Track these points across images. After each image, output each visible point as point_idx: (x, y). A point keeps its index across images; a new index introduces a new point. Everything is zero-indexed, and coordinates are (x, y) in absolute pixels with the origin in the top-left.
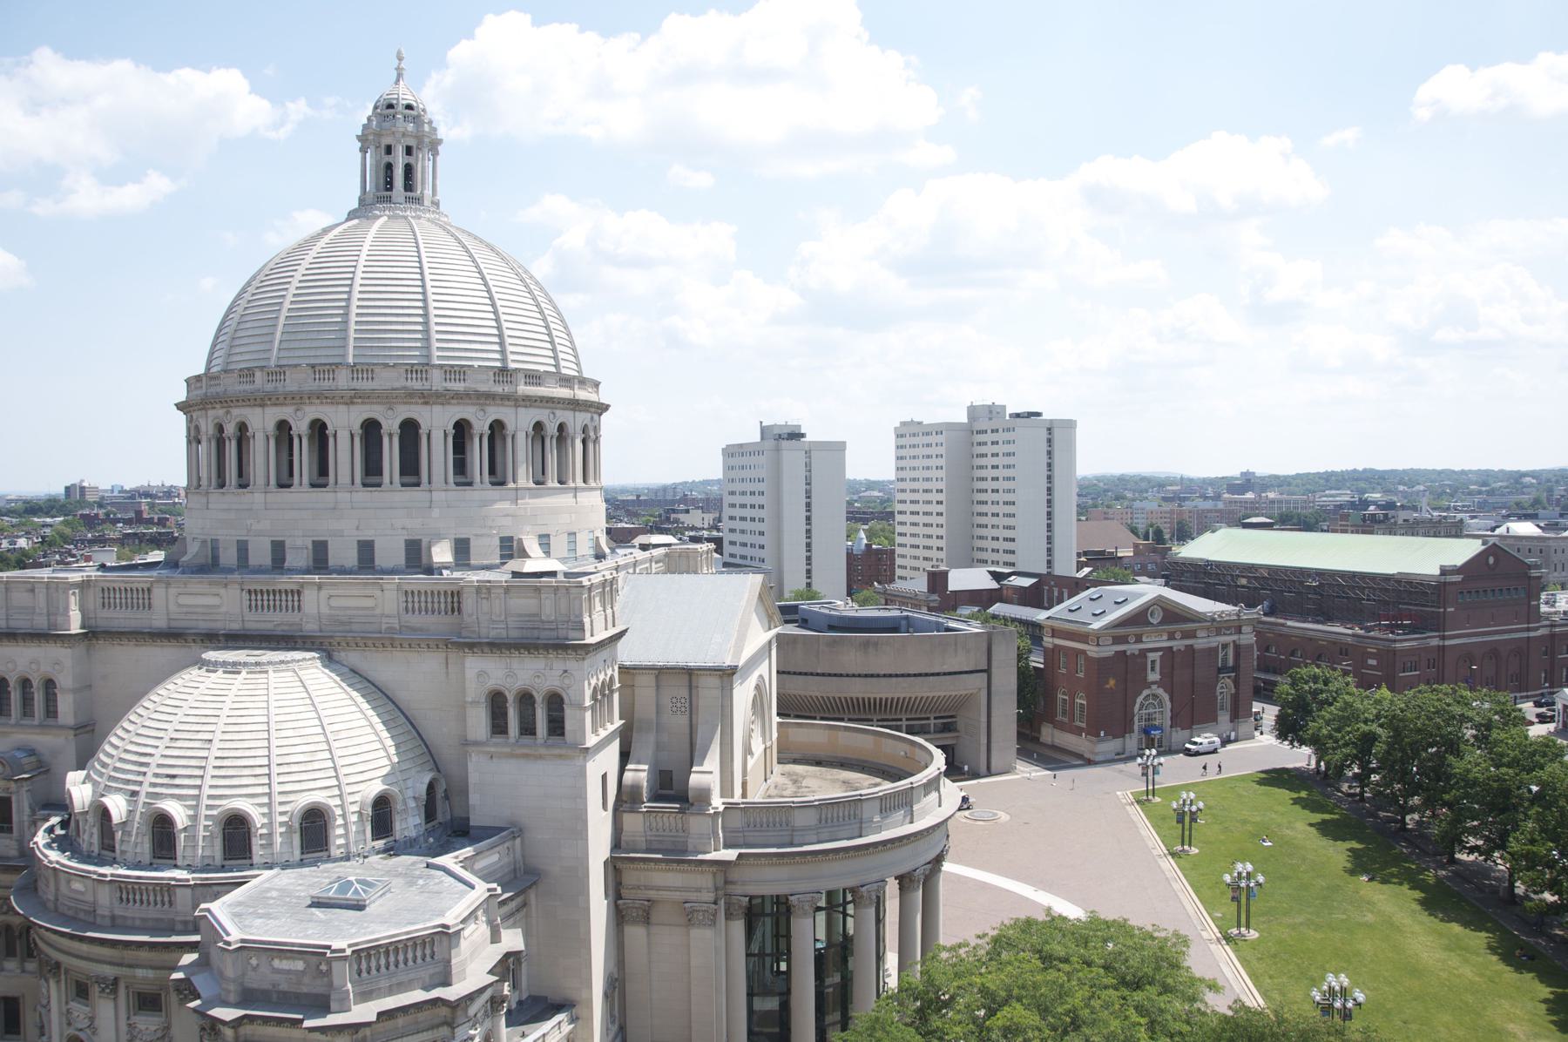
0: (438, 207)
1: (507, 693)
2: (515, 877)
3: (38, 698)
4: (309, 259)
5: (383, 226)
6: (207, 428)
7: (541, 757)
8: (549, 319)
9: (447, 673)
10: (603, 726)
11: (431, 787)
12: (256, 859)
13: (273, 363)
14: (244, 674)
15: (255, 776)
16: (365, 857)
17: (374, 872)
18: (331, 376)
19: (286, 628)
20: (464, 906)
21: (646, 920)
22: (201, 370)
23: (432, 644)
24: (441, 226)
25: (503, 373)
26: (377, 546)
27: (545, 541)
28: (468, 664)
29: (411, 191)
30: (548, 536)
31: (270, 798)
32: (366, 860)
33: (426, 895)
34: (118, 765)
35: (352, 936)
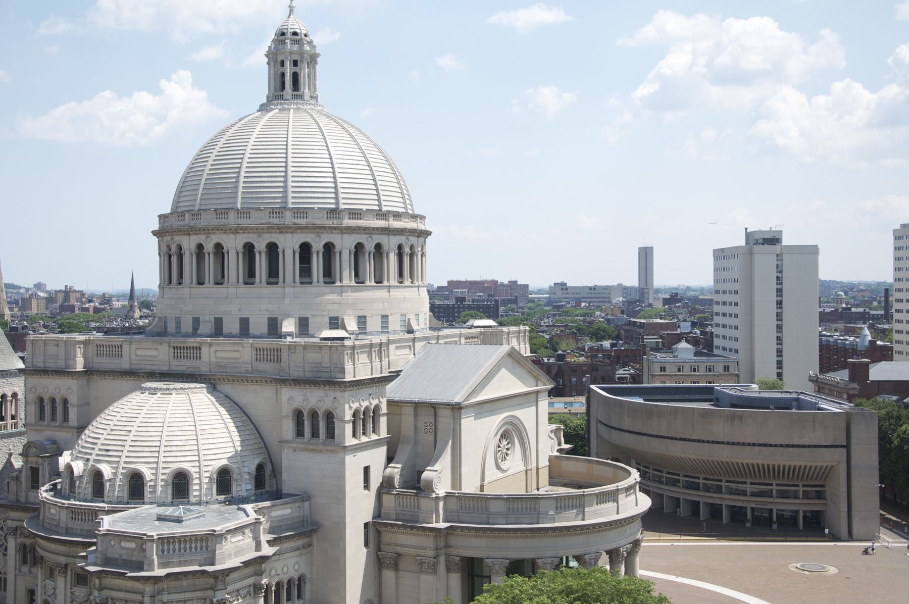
3: (59, 409)
7: (321, 451)
9: (277, 399)
11: (260, 468)
12: (146, 500)
13: (196, 208)
14: (159, 395)
15: (151, 452)
18: (226, 216)
19: (192, 370)
21: (396, 567)
26: (251, 321)
34: (84, 444)
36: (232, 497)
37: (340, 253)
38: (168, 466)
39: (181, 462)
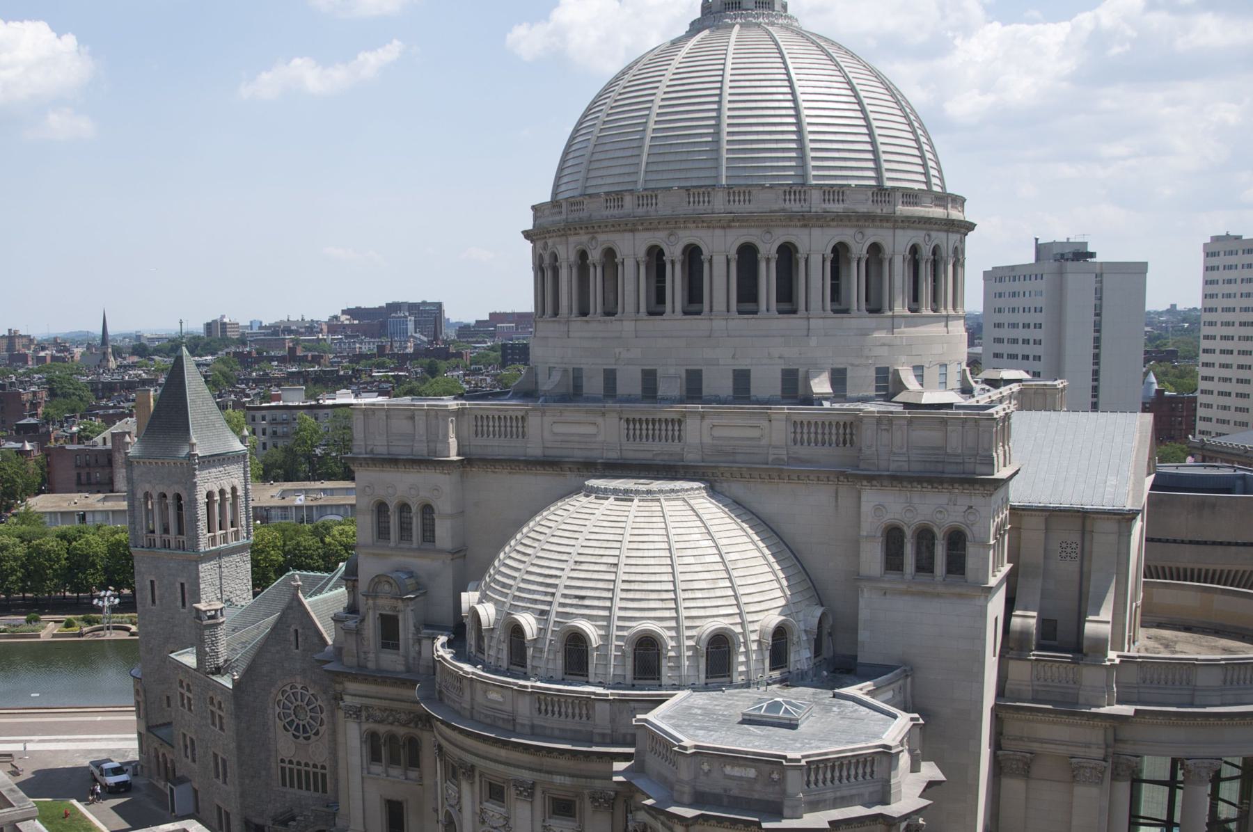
15: (662, 600)
18: (706, 199)
27: (919, 371)
36: (789, 672)
38: (694, 625)
39: (713, 616)
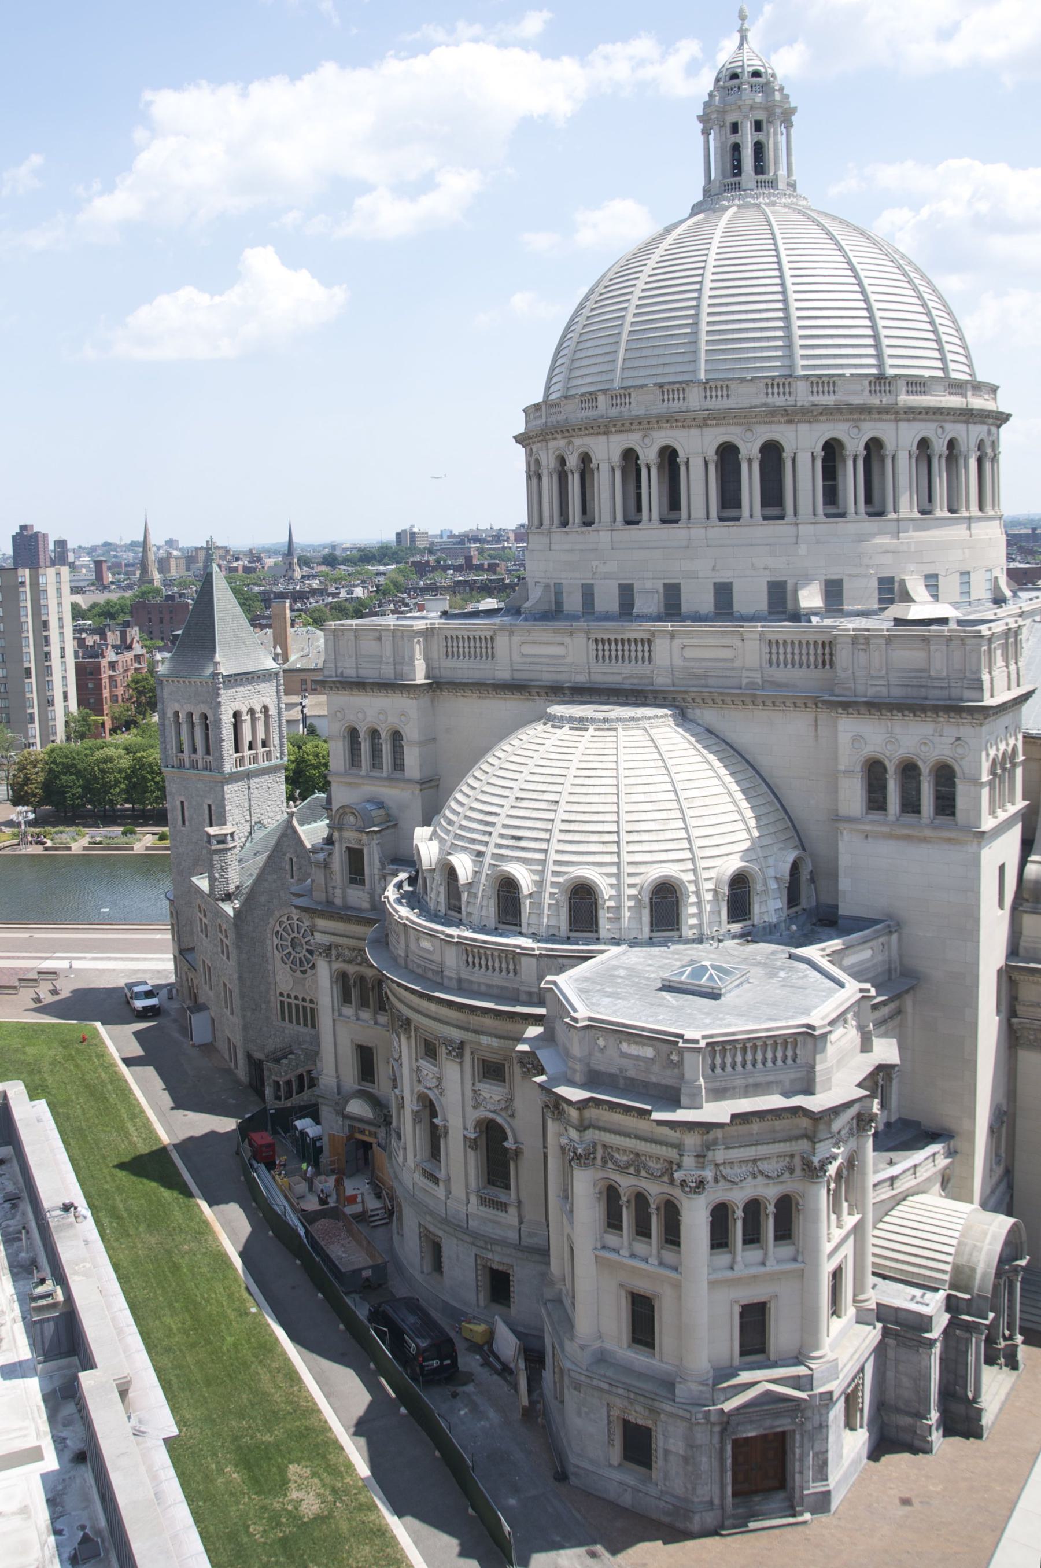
0: (795, 190)
1: (887, 763)
2: (890, 979)
3: (386, 749)
4: (651, 264)
5: (733, 217)
6: (548, 461)
7: (925, 840)
8: (934, 312)
9: (817, 736)
10: (1002, 807)
11: (795, 867)
12: (603, 933)
13: (616, 385)
14: (591, 731)
15: (603, 843)
16: (720, 941)
17: (729, 959)
18: (681, 396)
19: (635, 681)
20: (834, 1006)
22: (539, 398)
23: (799, 702)
24: (799, 212)
25: (881, 381)
26: (735, 589)
27: (932, 583)
28: (840, 728)
29: (762, 173)
30: (936, 576)
31: (619, 868)
32: (721, 944)
33: (789, 989)
34: (464, 823)
35: (706, 1026)
36: (753, 925)
37: (894, 457)
38: (638, 871)
